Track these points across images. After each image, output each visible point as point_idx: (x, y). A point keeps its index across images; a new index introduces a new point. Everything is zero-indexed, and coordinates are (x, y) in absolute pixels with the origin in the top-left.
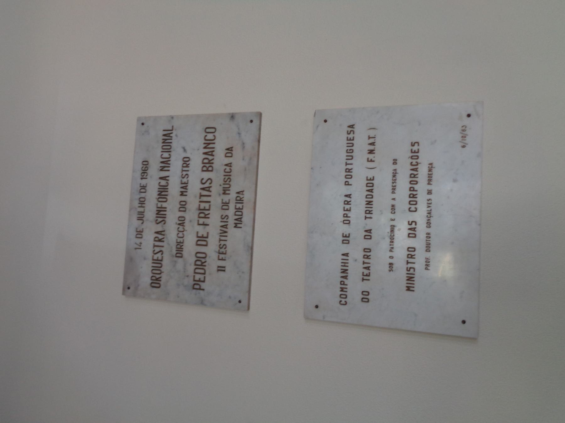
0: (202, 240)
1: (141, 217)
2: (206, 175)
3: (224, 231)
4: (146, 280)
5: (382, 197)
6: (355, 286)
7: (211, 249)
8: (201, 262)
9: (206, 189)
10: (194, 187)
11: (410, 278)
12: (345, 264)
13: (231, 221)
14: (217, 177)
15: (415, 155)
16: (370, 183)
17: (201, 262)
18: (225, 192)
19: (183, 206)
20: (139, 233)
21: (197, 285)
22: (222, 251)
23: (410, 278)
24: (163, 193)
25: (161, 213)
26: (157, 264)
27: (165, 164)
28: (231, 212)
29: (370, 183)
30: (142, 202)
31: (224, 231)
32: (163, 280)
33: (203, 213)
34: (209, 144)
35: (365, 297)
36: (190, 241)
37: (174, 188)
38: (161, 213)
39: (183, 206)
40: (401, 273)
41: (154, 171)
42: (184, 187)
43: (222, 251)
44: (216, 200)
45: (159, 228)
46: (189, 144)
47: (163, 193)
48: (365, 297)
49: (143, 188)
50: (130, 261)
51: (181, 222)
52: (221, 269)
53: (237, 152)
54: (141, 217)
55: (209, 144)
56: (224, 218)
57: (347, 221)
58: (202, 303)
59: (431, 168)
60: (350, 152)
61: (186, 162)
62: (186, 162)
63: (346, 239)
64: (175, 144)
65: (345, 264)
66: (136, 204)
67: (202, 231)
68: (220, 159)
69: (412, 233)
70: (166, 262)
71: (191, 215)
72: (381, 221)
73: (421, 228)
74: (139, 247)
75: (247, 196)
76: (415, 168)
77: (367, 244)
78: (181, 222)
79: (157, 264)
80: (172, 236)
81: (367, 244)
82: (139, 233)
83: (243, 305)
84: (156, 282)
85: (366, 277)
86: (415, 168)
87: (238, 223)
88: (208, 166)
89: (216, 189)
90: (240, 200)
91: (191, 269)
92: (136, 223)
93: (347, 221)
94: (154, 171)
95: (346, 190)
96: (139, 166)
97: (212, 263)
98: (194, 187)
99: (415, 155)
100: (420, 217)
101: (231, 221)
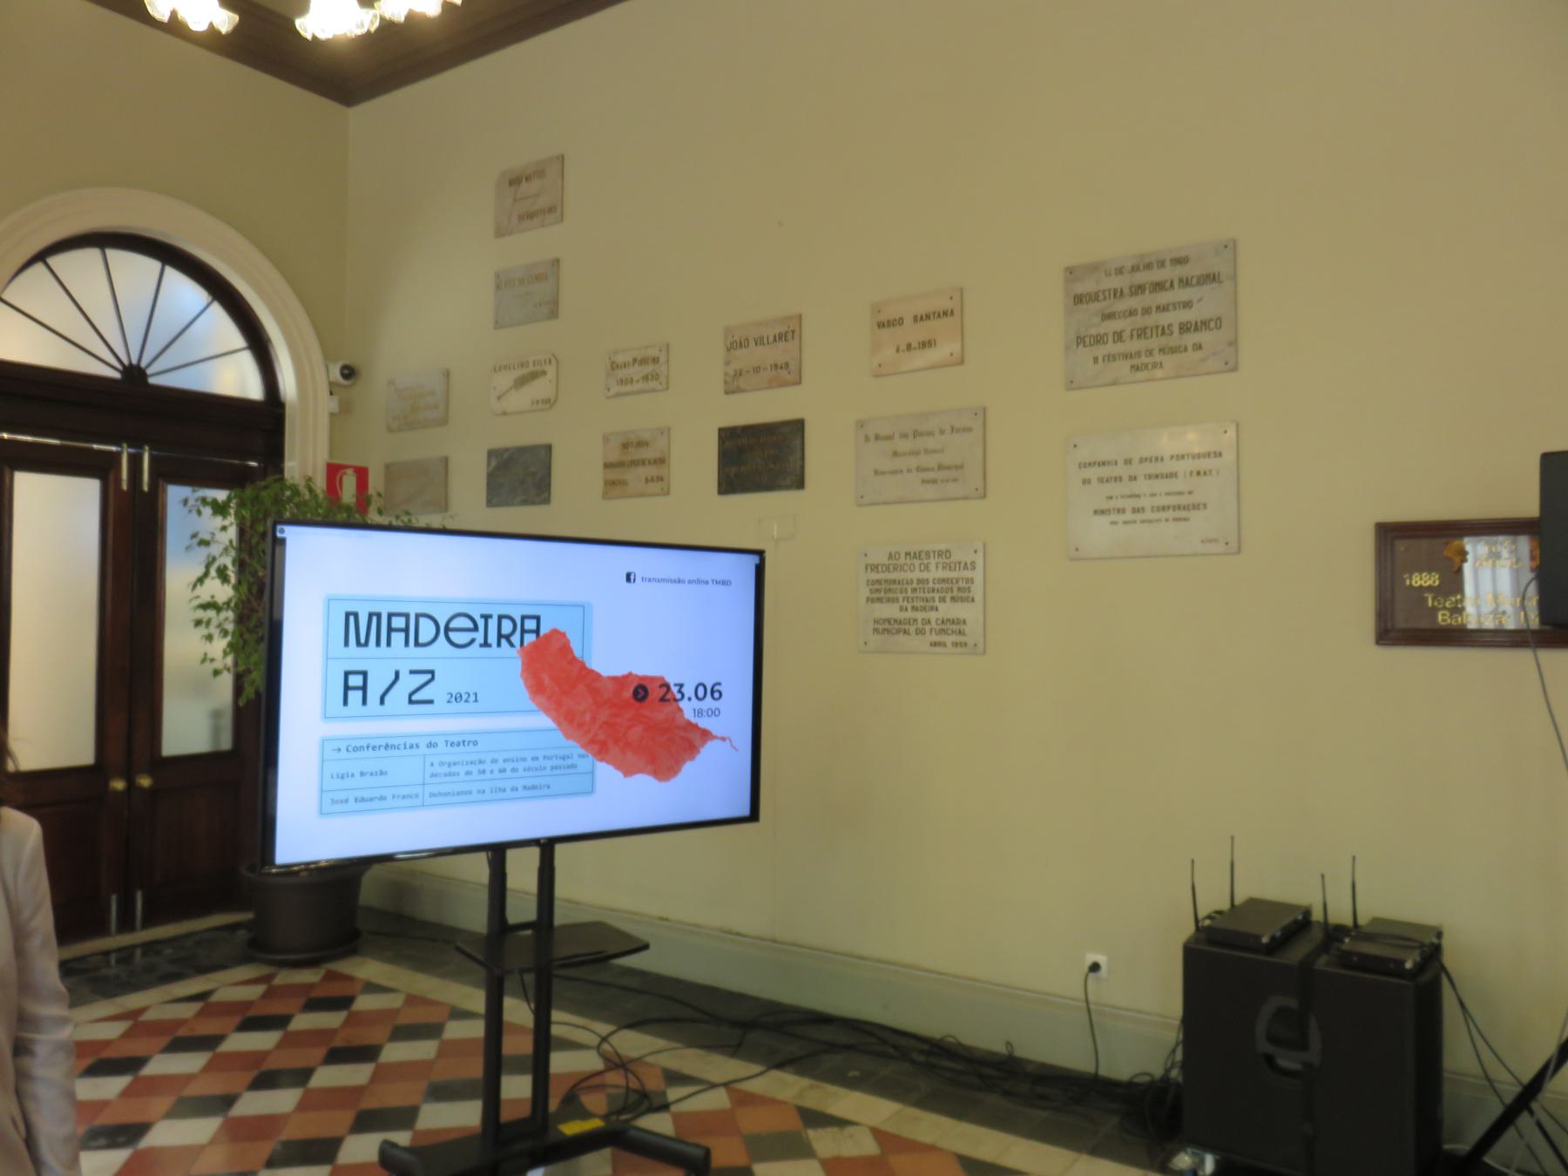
0: (1119, 336)
1: (1135, 269)
2: (1176, 329)
3: (1127, 356)
4: (1081, 288)
5: (1161, 486)
6: (1093, 473)
7: (1112, 347)
8: (1099, 340)
9: (1164, 331)
10: (1165, 319)
11: (1103, 512)
12: (1109, 463)
13: (1135, 361)
14: (1175, 339)
15: (1196, 507)
16: (1173, 475)
17: (1099, 340)
18: (1162, 350)
19: (1147, 311)
20: (1120, 271)
21: (1080, 340)
22: (1111, 358)
23: (1103, 512)
24: (1159, 286)
25: (1138, 289)
26: (1094, 297)
27: (1185, 282)
28: (1144, 359)
29: (1173, 475)
30: (1148, 266)
31: (1127, 356)
32: (1084, 306)
33: (1142, 333)
34: (1204, 325)
35: (1086, 482)
36: (1116, 325)
37: (1164, 298)
38: (1138, 289)
39: (1147, 311)
40: (1105, 505)
41: (1180, 271)
42: (1163, 309)
43: (1111, 358)
44: (1155, 342)
45: (1126, 291)
46: (1207, 303)
47: (1159, 286)
48: (1086, 482)
49: (1162, 264)
50: (1094, 268)
51: (1132, 313)
52: (1096, 360)
53: (1199, 354)
54: (1135, 269)
55: (1204, 325)
56: (1138, 354)
57: (1142, 460)
58: (1067, 348)
59: (1185, 519)
60: (1199, 456)
61: (1187, 305)
62: (1187, 305)
63: (1128, 462)
64: (1206, 290)
65: (1109, 463)
66: (1147, 260)
67: (1126, 335)
68: (1191, 339)
69: (1136, 510)
70: (1096, 306)
71: (1140, 321)
72: (1142, 486)
73: (1139, 517)
74: (1108, 274)
75: (1158, 373)
76: (1186, 508)
77: (1125, 478)
78: (1132, 313)
79: (1094, 297)
80: (1121, 305)
81: (1125, 478)
82: (1120, 271)
83: (1071, 385)
84: (1079, 299)
85: (1101, 480)
86: (1186, 508)
87: (1135, 368)
88: (1185, 328)
89: (1163, 341)
90: (1155, 366)
91: (1093, 332)
92: (1129, 265)
93: (1142, 460)
94: (1180, 271)
95: (1167, 458)
96: (1182, 254)
97: (1101, 351)
98: (1165, 319)
99: (1196, 507)
100: (1148, 515)
101: (1135, 361)
